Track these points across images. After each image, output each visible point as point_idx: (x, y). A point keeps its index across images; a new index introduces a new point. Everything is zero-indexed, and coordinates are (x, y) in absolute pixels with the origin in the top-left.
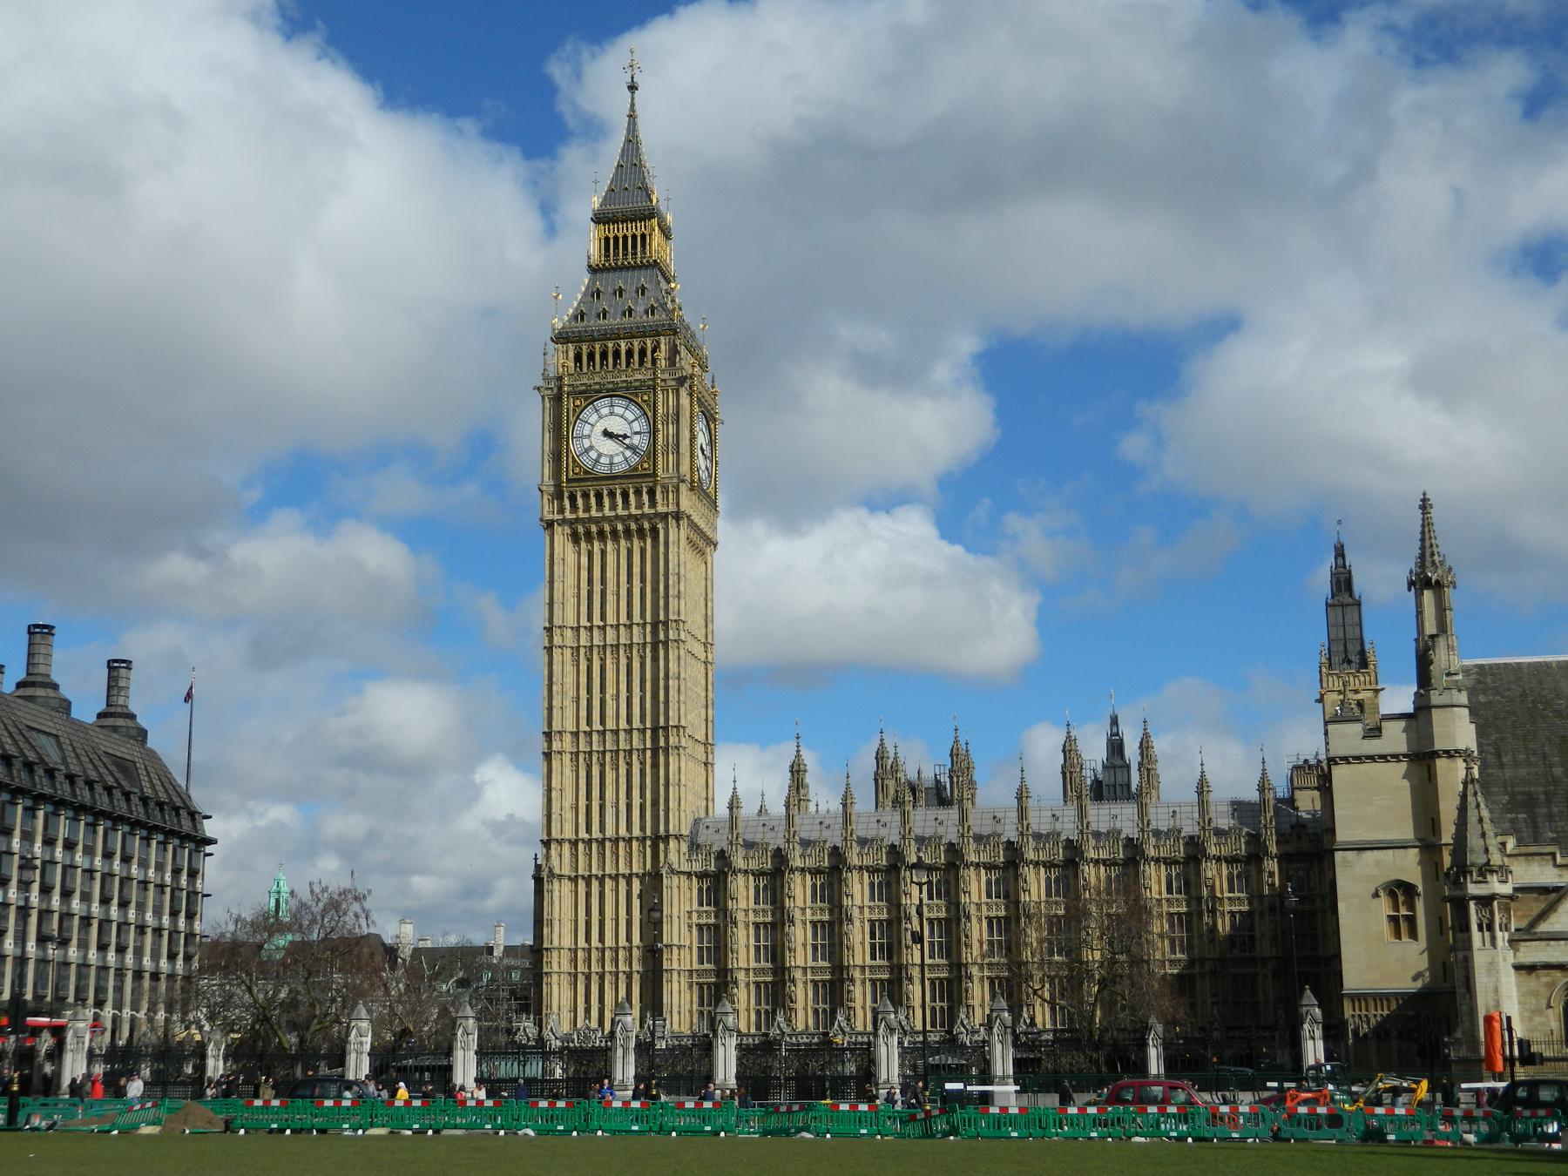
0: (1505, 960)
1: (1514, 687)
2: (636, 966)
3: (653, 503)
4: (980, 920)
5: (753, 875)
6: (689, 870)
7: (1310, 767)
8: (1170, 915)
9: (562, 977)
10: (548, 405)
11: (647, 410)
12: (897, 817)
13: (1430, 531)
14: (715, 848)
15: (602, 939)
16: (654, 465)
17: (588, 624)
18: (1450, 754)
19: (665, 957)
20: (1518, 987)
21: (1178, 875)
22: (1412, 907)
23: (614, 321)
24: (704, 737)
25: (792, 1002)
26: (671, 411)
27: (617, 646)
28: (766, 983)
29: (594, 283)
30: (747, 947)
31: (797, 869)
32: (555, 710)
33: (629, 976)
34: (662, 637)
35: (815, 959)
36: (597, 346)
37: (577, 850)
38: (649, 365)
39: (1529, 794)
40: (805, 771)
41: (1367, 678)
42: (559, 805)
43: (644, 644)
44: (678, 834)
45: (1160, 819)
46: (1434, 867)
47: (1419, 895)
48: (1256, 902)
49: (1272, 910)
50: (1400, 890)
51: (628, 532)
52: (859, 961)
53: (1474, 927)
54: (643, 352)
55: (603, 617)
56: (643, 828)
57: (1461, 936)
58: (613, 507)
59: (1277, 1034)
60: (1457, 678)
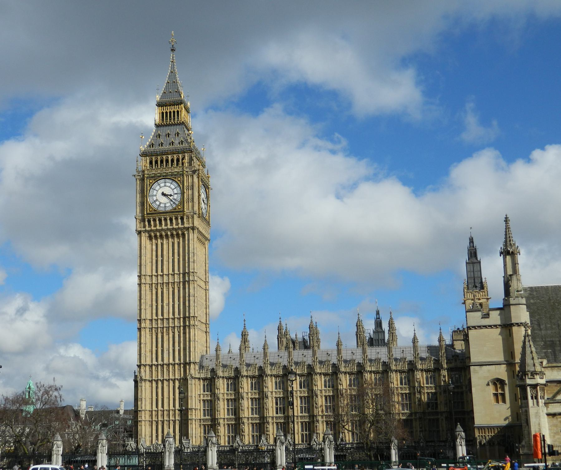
0: (543, 411)
1: (545, 296)
2: (178, 418)
3: (183, 223)
4: (322, 397)
6: (199, 377)
7: (460, 331)
8: (402, 394)
9: (146, 423)
10: (138, 182)
11: (180, 184)
12: (287, 354)
13: (509, 231)
14: (210, 368)
15: (163, 406)
17: (156, 274)
18: (518, 325)
19: (189, 414)
20: (548, 423)
21: (405, 377)
22: (503, 389)
23: (166, 147)
24: (205, 321)
25: (243, 432)
26: (190, 184)
27: (168, 283)
29: (158, 131)
30: (224, 409)
31: (244, 376)
32: (142, 310)
33: (174, 422)
34: (187, 279)
35: (252, 414)
36: (159, 158)
38: (181, 165)
39: (552, 341)
40: (248, 335)
41: (484, 294)
42: (144, 350)
43: (180, 282)
44: (194, 362)
45: (397, 354)
46: (512, 372)
47: (506, 384)
48: (438, 388)
49: (445, 391)
50: (498, 383)
51: (172, 235)
52: (271, 415)
53: (529, 398)
54: (178, 160)
55: (162, 271)
56: (180, 359)
57: (524, 401)
59: (447, 444)
60: (521, 293)
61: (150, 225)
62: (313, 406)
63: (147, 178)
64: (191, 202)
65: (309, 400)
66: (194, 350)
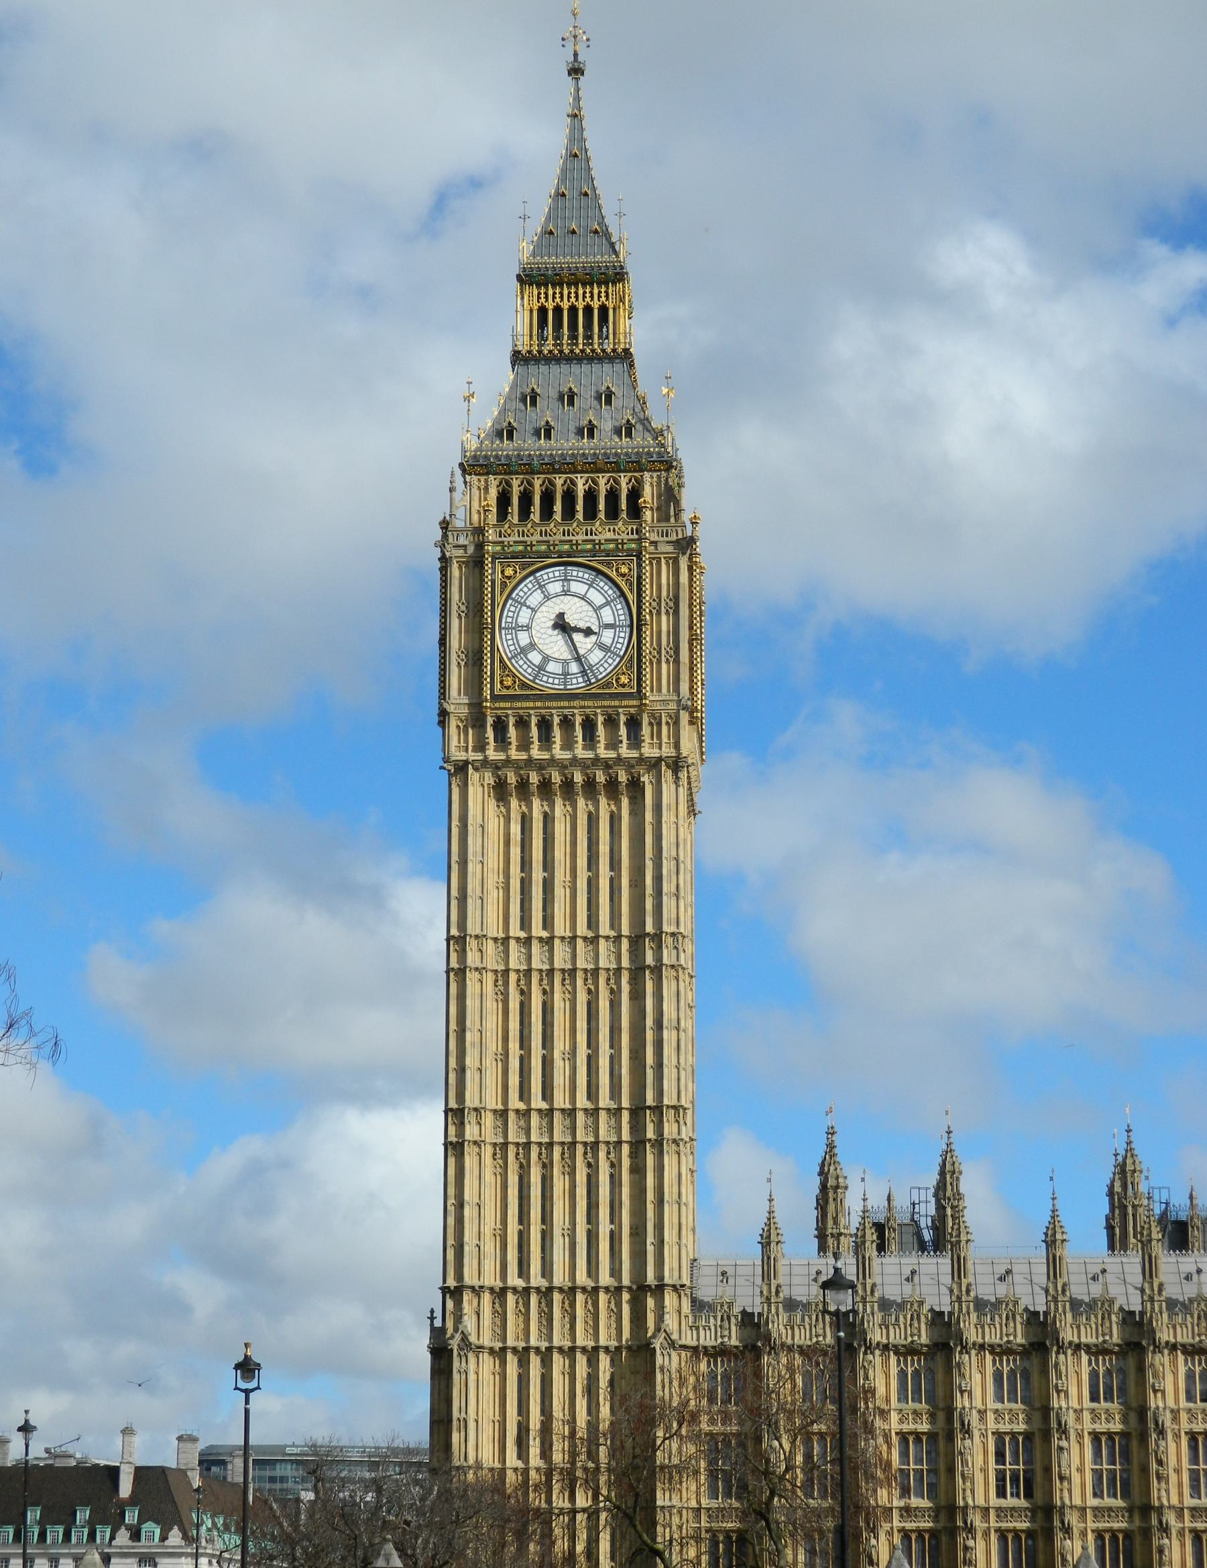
4: (1177, 1436)
6: (694, 1343)
16: (639, 680)
17: (523, 935)
23: (565, 444)
26: (664, 594)
27: (573, 972)
28: (920, 1532)
32: (468, 1074)
33: (593, 1514)
34: (649, 959)
37: (504, 1305)
40: (846, 1188)
43: (619, 970)
44: (678, 1283)
45: (986, 1288)
51: (590, 786)
52: (980, 1501)
54: (613, 496)
55: (548, 922)
56: (615, 1272)
58: (568, 745)
61: (502, 740)
62: (1145, 1469)
63: (494, 558)
64: (668, 661)
65: (1127, 1446)
66: (675, 1239)
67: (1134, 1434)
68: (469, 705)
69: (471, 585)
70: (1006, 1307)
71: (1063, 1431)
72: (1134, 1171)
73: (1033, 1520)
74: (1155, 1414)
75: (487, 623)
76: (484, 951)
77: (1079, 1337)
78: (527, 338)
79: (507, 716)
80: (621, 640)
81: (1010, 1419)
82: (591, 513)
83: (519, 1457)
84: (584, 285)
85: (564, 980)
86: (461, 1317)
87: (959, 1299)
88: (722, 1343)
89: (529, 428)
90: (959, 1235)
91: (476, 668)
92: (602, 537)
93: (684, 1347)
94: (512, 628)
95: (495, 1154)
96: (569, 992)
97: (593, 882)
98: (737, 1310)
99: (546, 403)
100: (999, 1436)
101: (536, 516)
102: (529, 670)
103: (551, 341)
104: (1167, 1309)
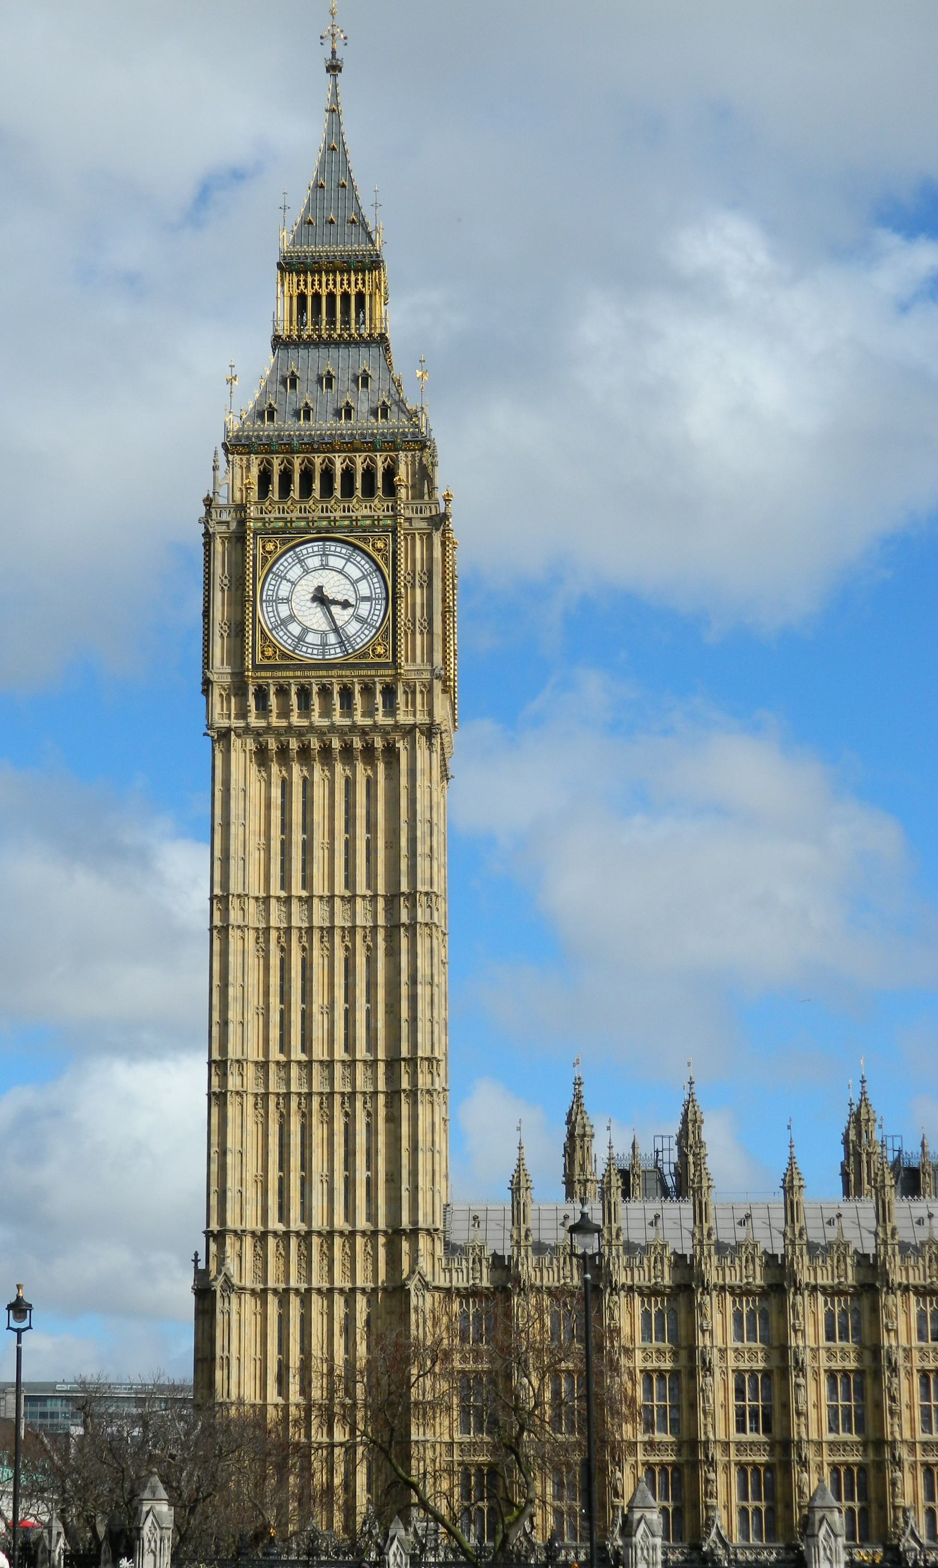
4: (909, 1373)
5: (640, 1295)
6: (447, 1285)
17: (283, 894)
25: (617, 1495)
26: (418, 568)
27: (331, 929)
28: (663, 1465)
34: (404, 918)
37: (265, 1248)
40: (593, 1136)
43: (375, 928)
44: (431, 1227)
51: (347, 752)
52: (721, 1436)
54: (369, 474)
55: (307, 882)
56: (372, 1217)
58: (326, 712)
61: (263, 708)
62: (878, 1405)
63: (255, 534)
64: (422, 633)
65: (862, 1382)
66: (429, 1185)
67: (868, 1371)
68: (232, 674)
69: (233, 559)
70: (746, 1250)
71: (801, 1369)
72: (868, 1120)
73: (771, 1453)
74: (888, 1352)
75: (249, 596)
76: (246, 910)
77: (816, 1279)
78: (287, 324)
79: (268, 685)
80: (377, 612)
81: (749, 1357)
82: (348, 491)
83: (280, 1394)
84: (342, 273)
85: (322, 937)
86: (224, 1259)
87: (701, 1242)
88: (474, 1285)
89: (289, 409)
90: (700, 1182)
91: (239, 639)
92: (359, 514)
93: (437, 1288)
94: (273, 601)
95: (256, 1104)
96: (327, 949)
97: (350, 844)
98: (488, 1253)
99: (306, 385)
100: (739, 1373)
101: (295, 494)
102: (289, 641)
103: (310, 326)
104: (900, 1252)
